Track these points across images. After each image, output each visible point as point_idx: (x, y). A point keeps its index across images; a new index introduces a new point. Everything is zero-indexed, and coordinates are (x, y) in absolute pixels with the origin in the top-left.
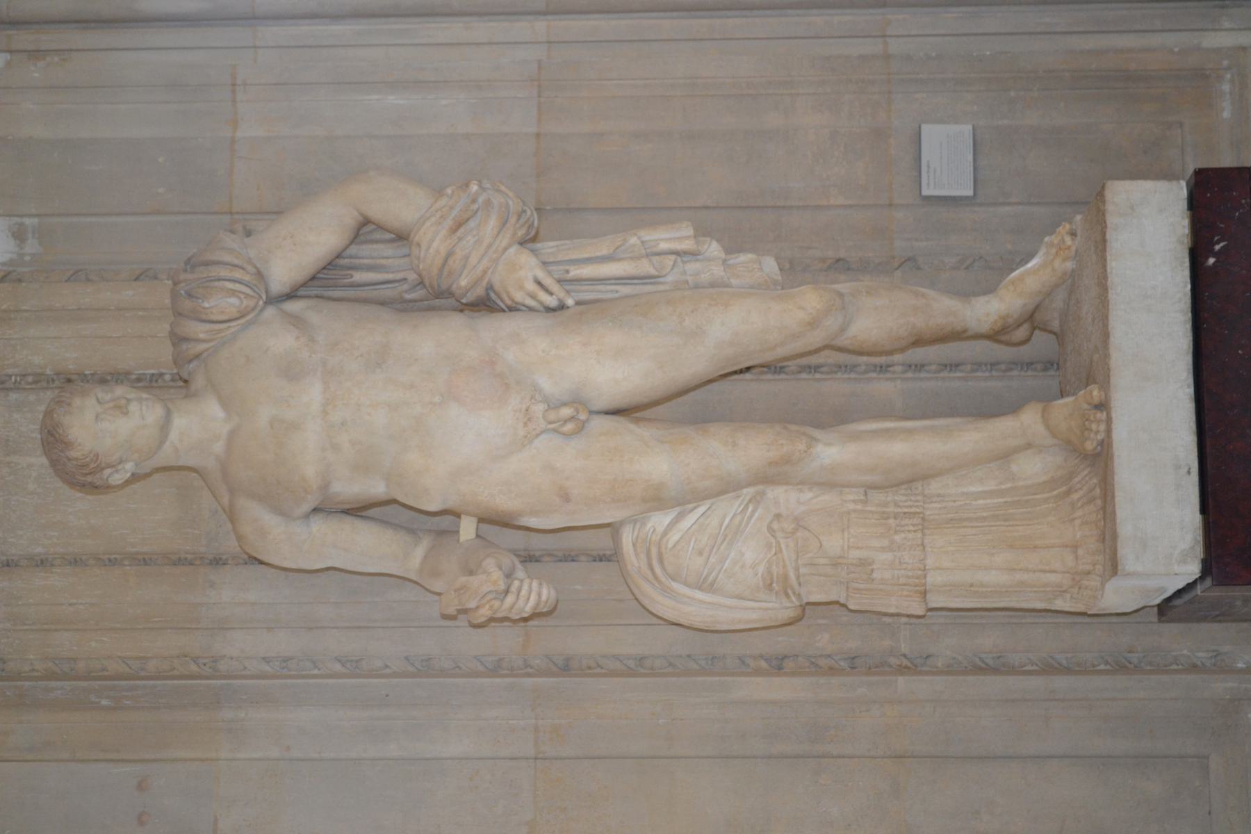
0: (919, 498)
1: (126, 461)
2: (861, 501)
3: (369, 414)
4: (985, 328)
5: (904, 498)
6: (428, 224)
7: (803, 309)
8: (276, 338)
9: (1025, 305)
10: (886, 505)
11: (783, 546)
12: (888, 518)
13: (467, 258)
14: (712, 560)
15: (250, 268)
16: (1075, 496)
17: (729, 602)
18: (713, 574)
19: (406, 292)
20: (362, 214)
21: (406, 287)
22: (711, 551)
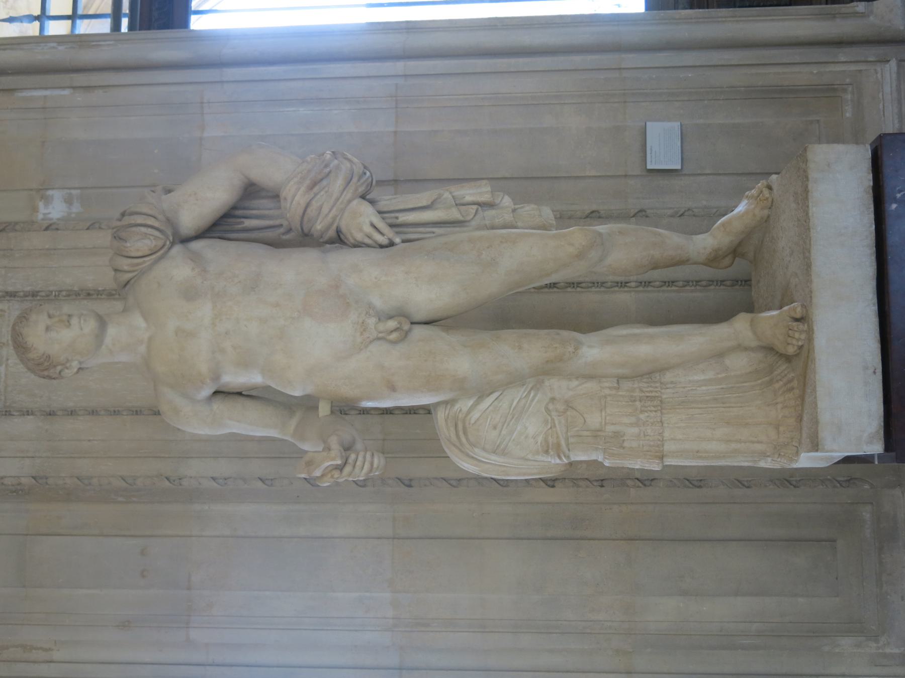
0: (658, 385)
2: (615, 388)
5: (646, 385)
6: (292, 183)
8: (178, 268)
11: (556, 422)
12: (635, 401)
13: (321, 208)
14: (504, 432)
15: (160, 217)
16: (777, 386)
19: (283, 234)
21: (282, 230)
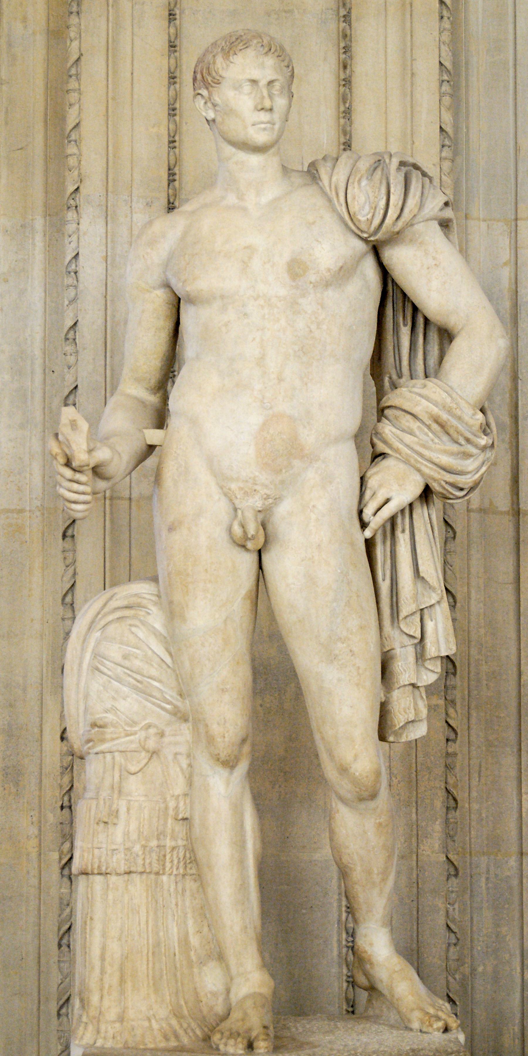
0: (181, 871)
1: (216, 111)
2: (177, 814)
3: (254, 339)
4: (361, 942)
5: (181, 855)
6: (445, 395)
7: (355, 760)
8: (333, 248)
9: (382, 981)
10: (173, 838)
11: (132, 738)
12: (158, 839)
13: (411, 433)
14: (119, 669)
15: (400, 224)
16: (174, 1022)
17: (82, 684)
18: (105, 670)
19: (390, 378)
20: (167, 279)
21: (394, 377)
22: (127, 669)
